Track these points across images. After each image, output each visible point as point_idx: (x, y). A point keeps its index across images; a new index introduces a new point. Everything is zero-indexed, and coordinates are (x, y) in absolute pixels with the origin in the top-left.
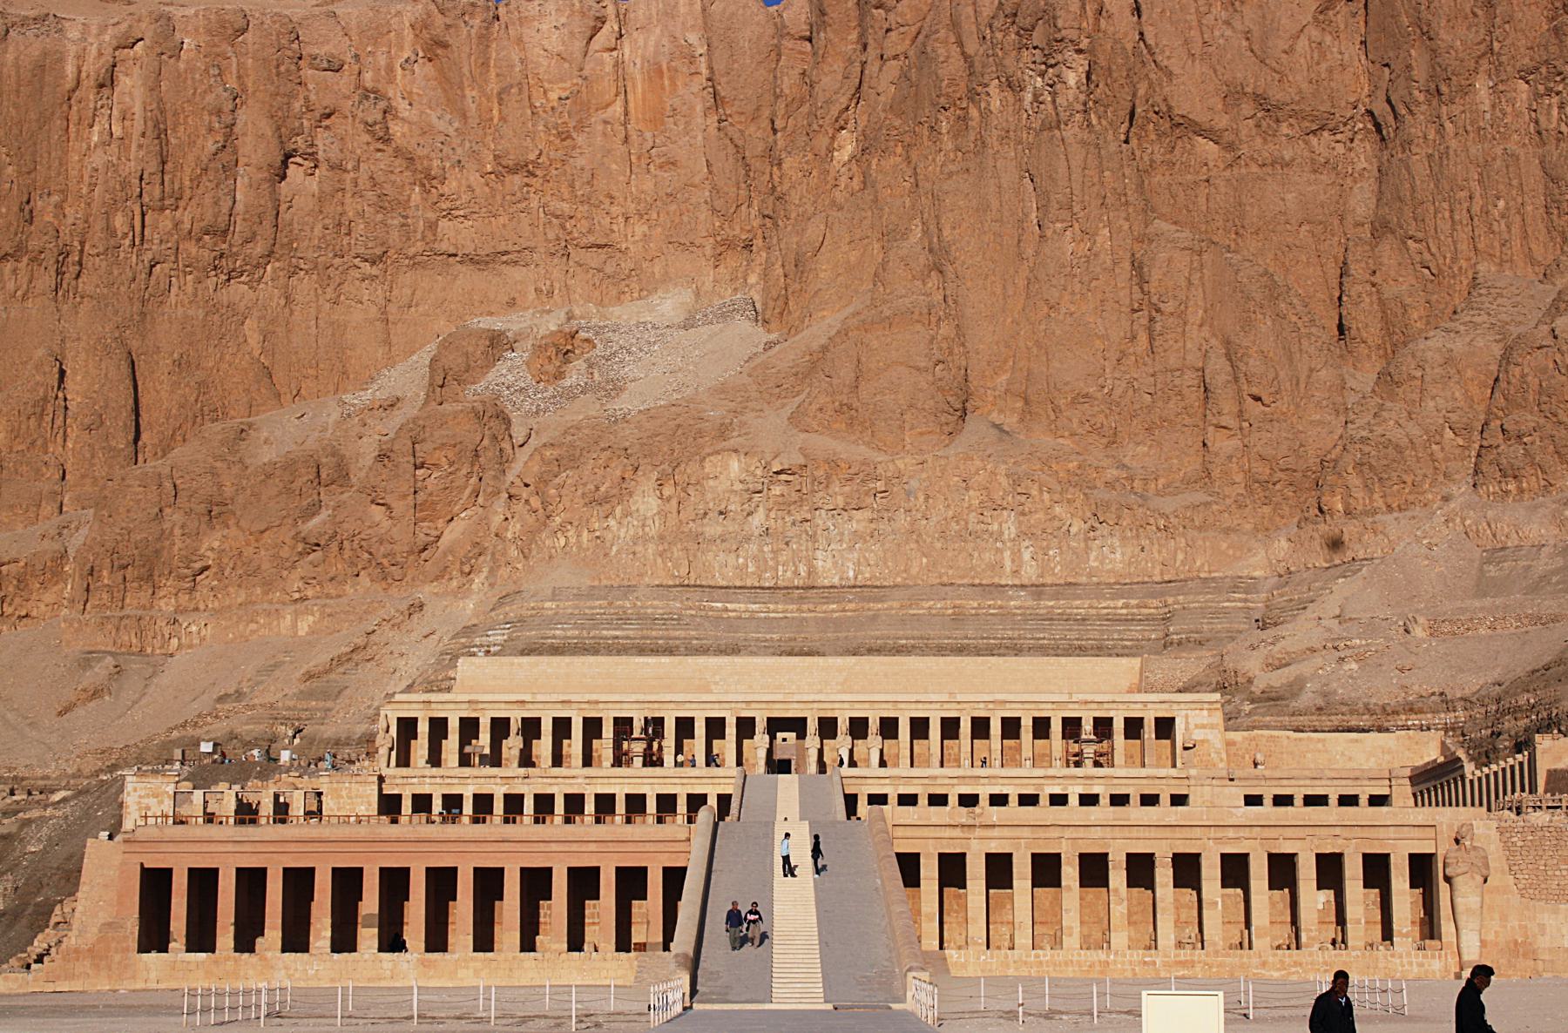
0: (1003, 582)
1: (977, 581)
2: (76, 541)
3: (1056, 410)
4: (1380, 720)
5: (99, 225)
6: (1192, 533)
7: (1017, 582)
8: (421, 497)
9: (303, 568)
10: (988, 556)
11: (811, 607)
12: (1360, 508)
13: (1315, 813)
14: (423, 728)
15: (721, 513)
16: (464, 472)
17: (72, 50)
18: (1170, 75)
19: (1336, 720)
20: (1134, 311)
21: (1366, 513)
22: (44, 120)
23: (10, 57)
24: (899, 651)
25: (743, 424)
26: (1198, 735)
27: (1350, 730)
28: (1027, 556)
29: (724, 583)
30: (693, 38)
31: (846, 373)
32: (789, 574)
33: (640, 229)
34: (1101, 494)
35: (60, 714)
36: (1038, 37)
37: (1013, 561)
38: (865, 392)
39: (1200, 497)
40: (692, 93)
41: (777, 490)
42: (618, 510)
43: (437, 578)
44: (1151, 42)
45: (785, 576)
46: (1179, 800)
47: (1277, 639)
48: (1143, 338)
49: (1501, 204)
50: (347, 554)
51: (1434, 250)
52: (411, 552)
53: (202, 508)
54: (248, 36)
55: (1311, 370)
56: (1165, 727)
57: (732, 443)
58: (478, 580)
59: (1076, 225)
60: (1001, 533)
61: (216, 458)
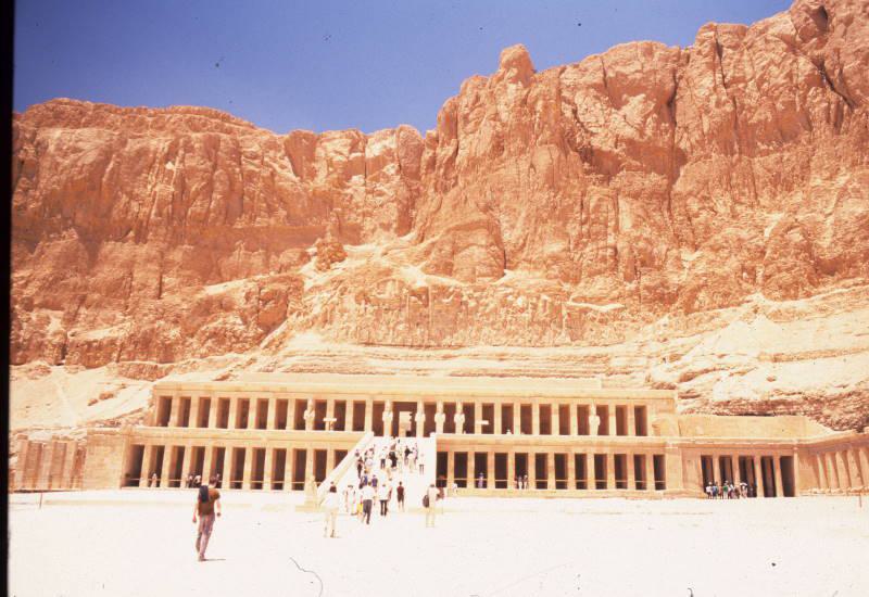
2: (122, 333)
3: (548, 266)
4: (765, 409)
5: (153, 212)
6: (618, 322)
9: (209, 343)
12: (706, 307)
14: (176, 404)
17: (152, 148)
18: (592, 134)
20: (582, 223)
21: (708, 309)
22: (139, 173)
23: (127, 149)
24: (474, 375)
27: (747, 414)
30: (394, 146)
31: (448, 248)
33: (369, 219)
34: (570, 303)
36: (539, 106)
38: (457, 260)
39: (618, 305)
40: (390, 169)
41: (413, 298)
44: (582, 120)
47: (684, 366)
52: (254, 338)
53: (172, 319)
54: (222, 144)
55: (668, 250)
56: (640, 412)
57: (394, 277)
61: (183, 300)
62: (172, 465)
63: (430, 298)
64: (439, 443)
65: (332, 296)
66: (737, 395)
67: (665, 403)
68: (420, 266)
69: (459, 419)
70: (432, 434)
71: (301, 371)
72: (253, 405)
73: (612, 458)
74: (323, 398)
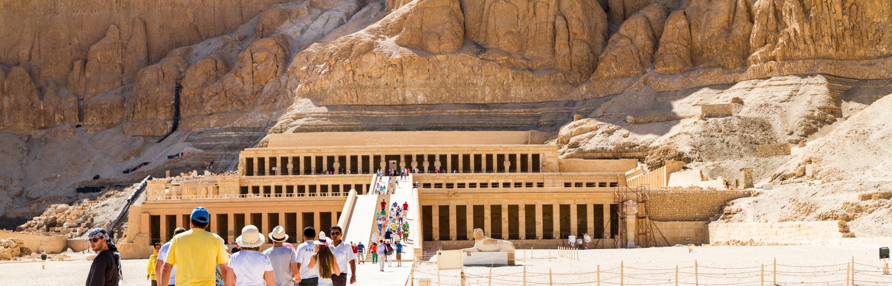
8: (255, 74)
9: (212, 102)
10: (472, 93)
13: (579, 189)
14: (256, 162)
19: (599, 155)
25: (377, 43)
26: (548, 160)
28: (487, 93)
41: (390, 69)
43: (263, 104)
45: (395, 100)
46: (540, 185)
48: (532, 10)
56: (536, 157)
58: (278, 104)
63: (405, 67)
64: (414, 179)
65: (325, 67)
66: (600, 146)
68: (395, 38)
69: (426, 165)
71: (307, 131)
72: (302, 160)
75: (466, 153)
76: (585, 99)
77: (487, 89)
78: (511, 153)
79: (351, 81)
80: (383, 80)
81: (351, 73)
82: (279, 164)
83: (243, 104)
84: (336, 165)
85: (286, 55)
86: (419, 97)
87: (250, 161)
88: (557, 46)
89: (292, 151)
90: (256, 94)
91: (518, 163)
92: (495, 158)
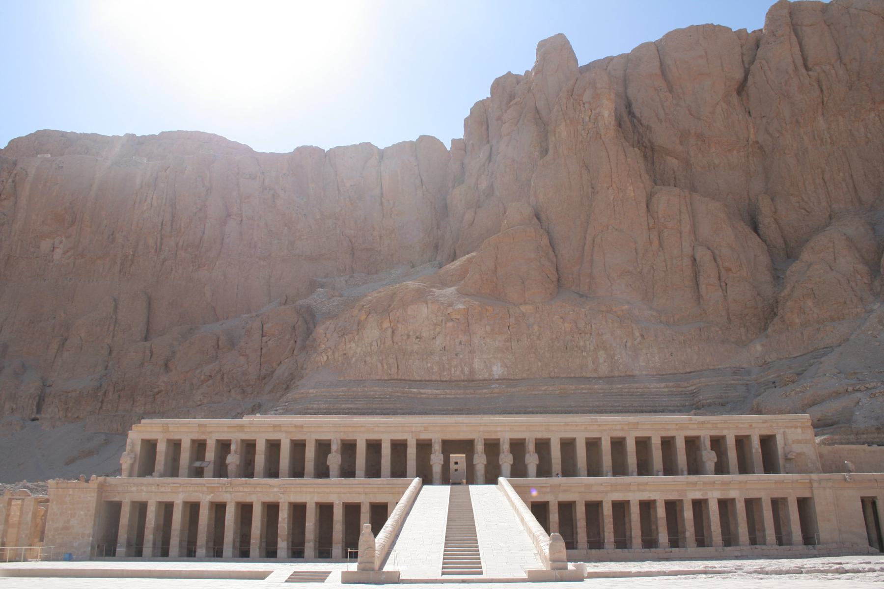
0: (588, 376)
1: (573, 375)
7: (596, 375)
8: (264, 351)
11: (472, 391)
14: (161, 448)
15: (417, 338)
16: (287, 337)
26: (797, 448)
28: (601, 360)
29: (419, 378)
32: (458, 372)
35: (67, 464)
37: (594, 363)
41: (450, 324)
42: (356, 338)
45: (456, 373)
49: (841, 174)
50: (225, 379)
51: (806, 200)
56: (767, 442)
59: (614, 185)
60: (585, 347)
62: (157, 528)
67: (799, 430)
70: (501, 479)
72: (261, 447)
73: (743, 504)
74: (350, 437)
75: (620, 434)
76: (766, 363)
77: (602, 355)
78: (715, 433)
79: (389, 342)
80: (438, 342)
81: (389, 331)
82: (210, 455)
83: (244, 392)
84: (334, 460)
85: (308, 328)
86: (495, 368)
87: (150, 446)
88: (703, 287)
89: (241, 427)
90: (263, 378)
91: (732, 455)
92: (680, 445)
